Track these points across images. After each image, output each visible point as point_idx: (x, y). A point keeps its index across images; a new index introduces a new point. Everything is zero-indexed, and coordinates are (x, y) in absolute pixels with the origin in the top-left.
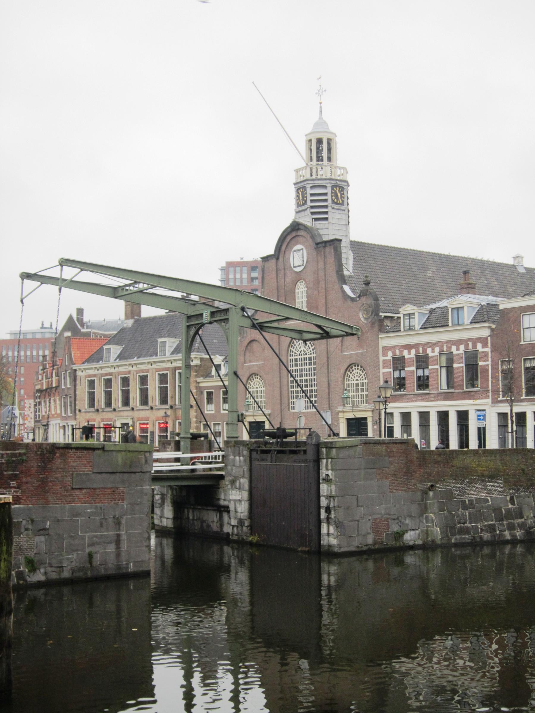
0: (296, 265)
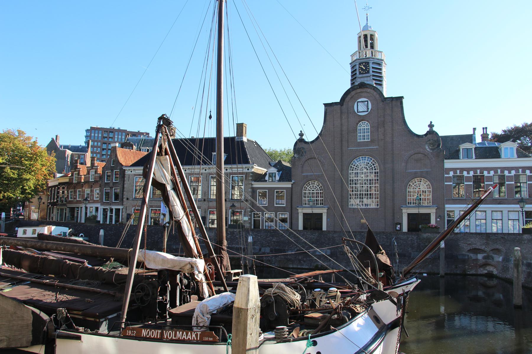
0: (360, 110)
